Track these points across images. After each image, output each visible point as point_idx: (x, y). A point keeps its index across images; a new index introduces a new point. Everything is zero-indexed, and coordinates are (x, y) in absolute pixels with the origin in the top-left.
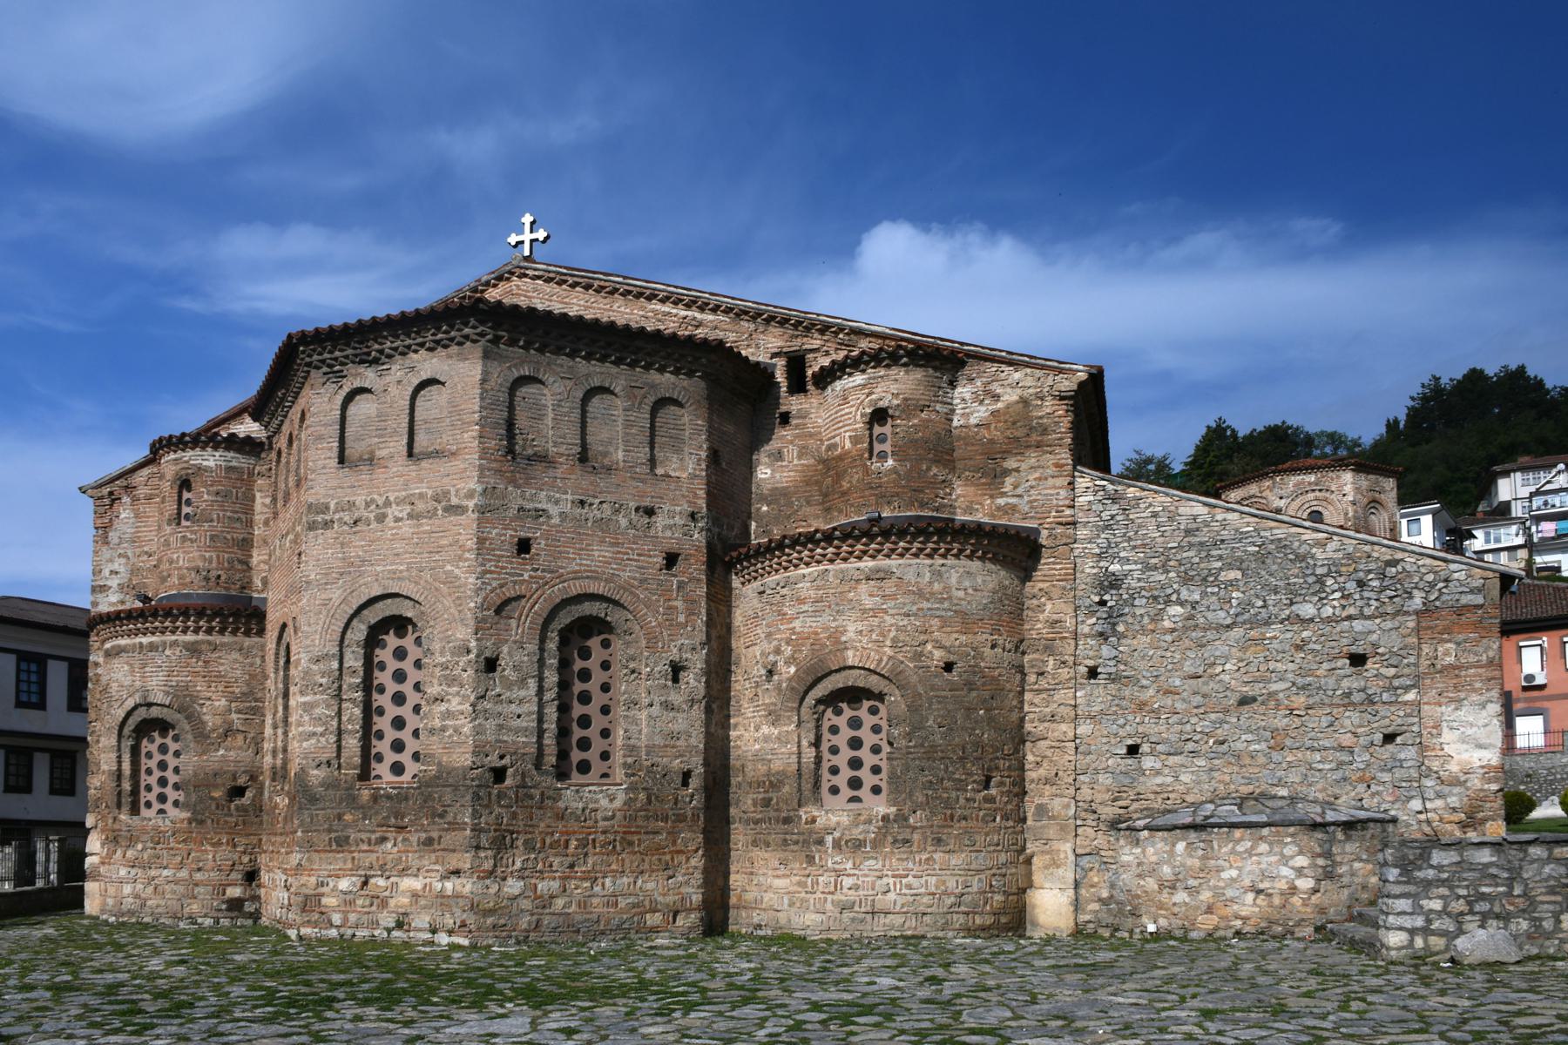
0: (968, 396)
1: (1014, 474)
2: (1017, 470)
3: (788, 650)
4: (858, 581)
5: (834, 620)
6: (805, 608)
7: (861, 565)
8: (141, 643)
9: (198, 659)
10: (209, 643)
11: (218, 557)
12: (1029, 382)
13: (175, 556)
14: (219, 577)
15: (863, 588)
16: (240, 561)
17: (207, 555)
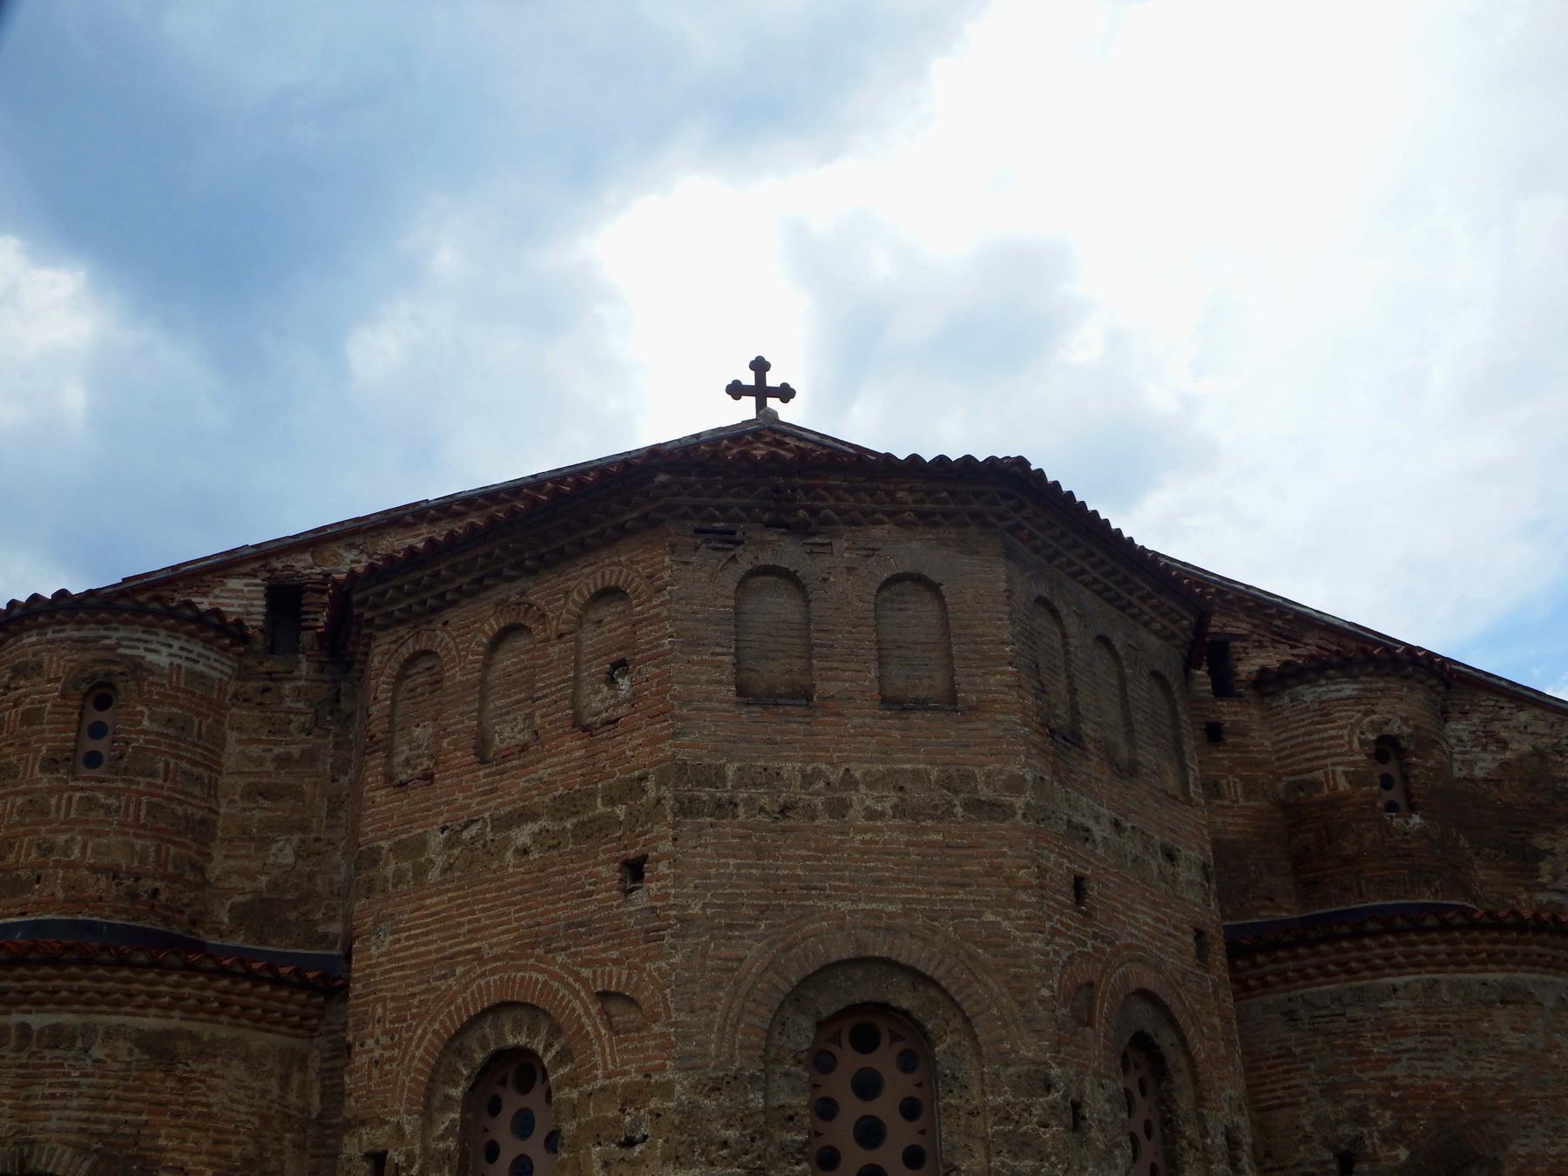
0: (1465, 736)
1: (1550, 858)
2: (1551, 852)
3: (1387, 1119)
4: (1489, 1004)
5: (1467, 1068)
6: (1408, 1043)
7: (1489, 977)
8: (24, 1029)
9: (168, 1072)
10: (193, 1037)
11: (158, 851)
12: (1541, 728)
13: (61, 839)
14: (156, 892)
15: (1501, 1016)
16: (195, 867)
17: (139, 843)
